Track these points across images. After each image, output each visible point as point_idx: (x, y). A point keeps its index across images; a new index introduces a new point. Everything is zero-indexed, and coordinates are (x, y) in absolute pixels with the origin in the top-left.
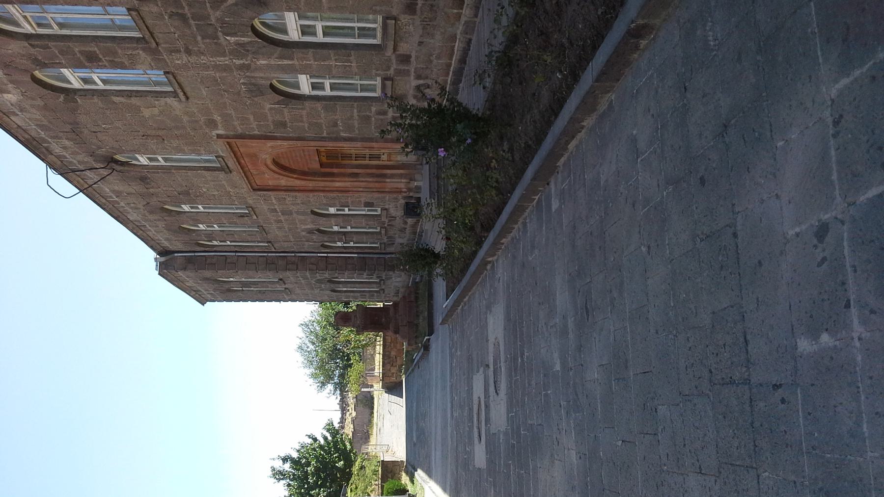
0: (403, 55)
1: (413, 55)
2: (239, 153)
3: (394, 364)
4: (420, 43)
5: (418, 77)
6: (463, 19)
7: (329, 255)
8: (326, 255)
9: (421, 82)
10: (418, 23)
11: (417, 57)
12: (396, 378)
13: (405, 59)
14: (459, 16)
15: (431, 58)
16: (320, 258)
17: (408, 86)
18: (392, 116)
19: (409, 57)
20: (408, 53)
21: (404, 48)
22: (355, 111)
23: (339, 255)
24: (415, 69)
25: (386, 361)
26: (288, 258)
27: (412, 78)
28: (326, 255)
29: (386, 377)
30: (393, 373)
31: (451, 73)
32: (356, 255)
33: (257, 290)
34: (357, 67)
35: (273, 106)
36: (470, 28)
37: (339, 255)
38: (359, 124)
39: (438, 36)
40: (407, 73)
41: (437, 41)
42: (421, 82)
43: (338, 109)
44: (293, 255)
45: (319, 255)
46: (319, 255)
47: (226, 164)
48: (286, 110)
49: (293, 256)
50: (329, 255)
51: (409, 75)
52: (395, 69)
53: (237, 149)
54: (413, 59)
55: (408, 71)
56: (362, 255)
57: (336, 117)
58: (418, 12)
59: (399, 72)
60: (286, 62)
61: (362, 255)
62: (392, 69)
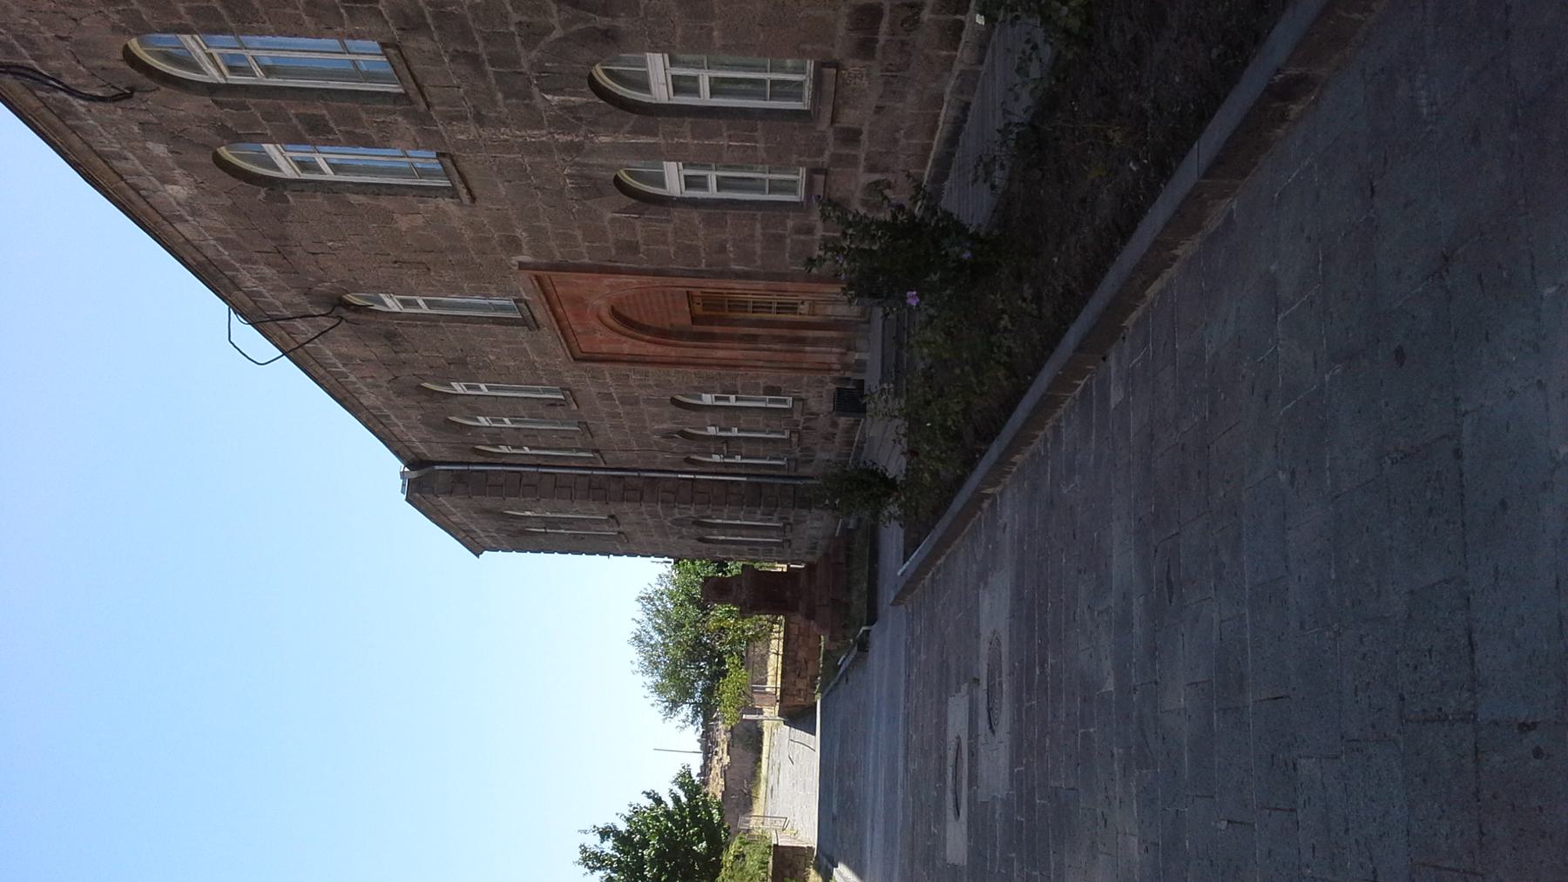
0: (847, 130)
1: (865, 129)
3: (803, 674)
4: (879, 109)
5: (872, 169)
6: (957, 67)
7: (697, 477)
8: (692, 477)
9: (876, 177)
11: (872, 133)
12: (805, 699)
13: (850, 136)
14: (951, 59)
15: (897, 135)
16: (681, 481)
18: (823, 236)
19: (859, 132)
20: (856, 126)
21: (849, 117)
22: (758, 226)
23: (715, 478)
25: (788, 668)
26: (627, 480)
27: (861, 169)
28: (692, 477)
29: (788, 696)
30: (800, 690)
31: (930, 163)
32: (745, 479)
33: (570, 534)
35: (617, 215)
36: (968, 81)
37: (715, 478)
39: (911, 98)
40: (853, 161)
42: (876, 177)
43: (729, 222)
44: (636, 474)
45: (680, 476)
46: (680, 476)
47: (530, 311)
48: (638, 223)
49: (635, 477)
50: (697, 477)
52: (832, 155)
54: (864, 137)
55: (855, 157)
56: (753, 479)
58: (878, 55)
59: (837, 159)
60: (643, 140)
61: (753, 479)
62: (827, 153)
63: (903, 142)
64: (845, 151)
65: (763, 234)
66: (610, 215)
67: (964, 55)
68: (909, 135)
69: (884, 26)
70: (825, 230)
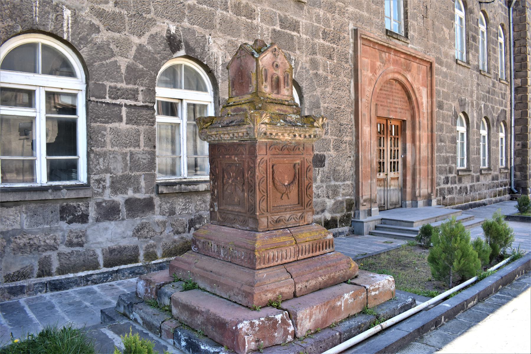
0: (479, 178)
1: (480, 183)
2: (412, 60)
4: (484, 185)
5: (471, 187)
6: (492, 199)
9: (469, 189)
10: (490, 182)
11: (479, 184)
13: (478, 180)
14: (491, 197)
17: (466, 183)
19: (479, 181)
21: (482, 178)
22: (452, 155)
24: (474, 185)
27: (471, 184)
31: (473, 202)
34: (474, 158)
35: (453, 107)
38: (443, 156)
40: (472, 182)
41: (484, 191)
42: (469, 189)
43: (453, 145)
47: (401, 41)
48: (449, 113)
51: (472, 182)
53: (418, 62)
54: (478, 183)
55: (473, 182)
57: (447, 142)
60: (475, 125)
63: (477, 193)
64: (475, 178)
65: (449, 156)
66: (453, 105)
67: (494, 199)
68: (479, 194)
69: (496, 181)
70: (451, 178)
